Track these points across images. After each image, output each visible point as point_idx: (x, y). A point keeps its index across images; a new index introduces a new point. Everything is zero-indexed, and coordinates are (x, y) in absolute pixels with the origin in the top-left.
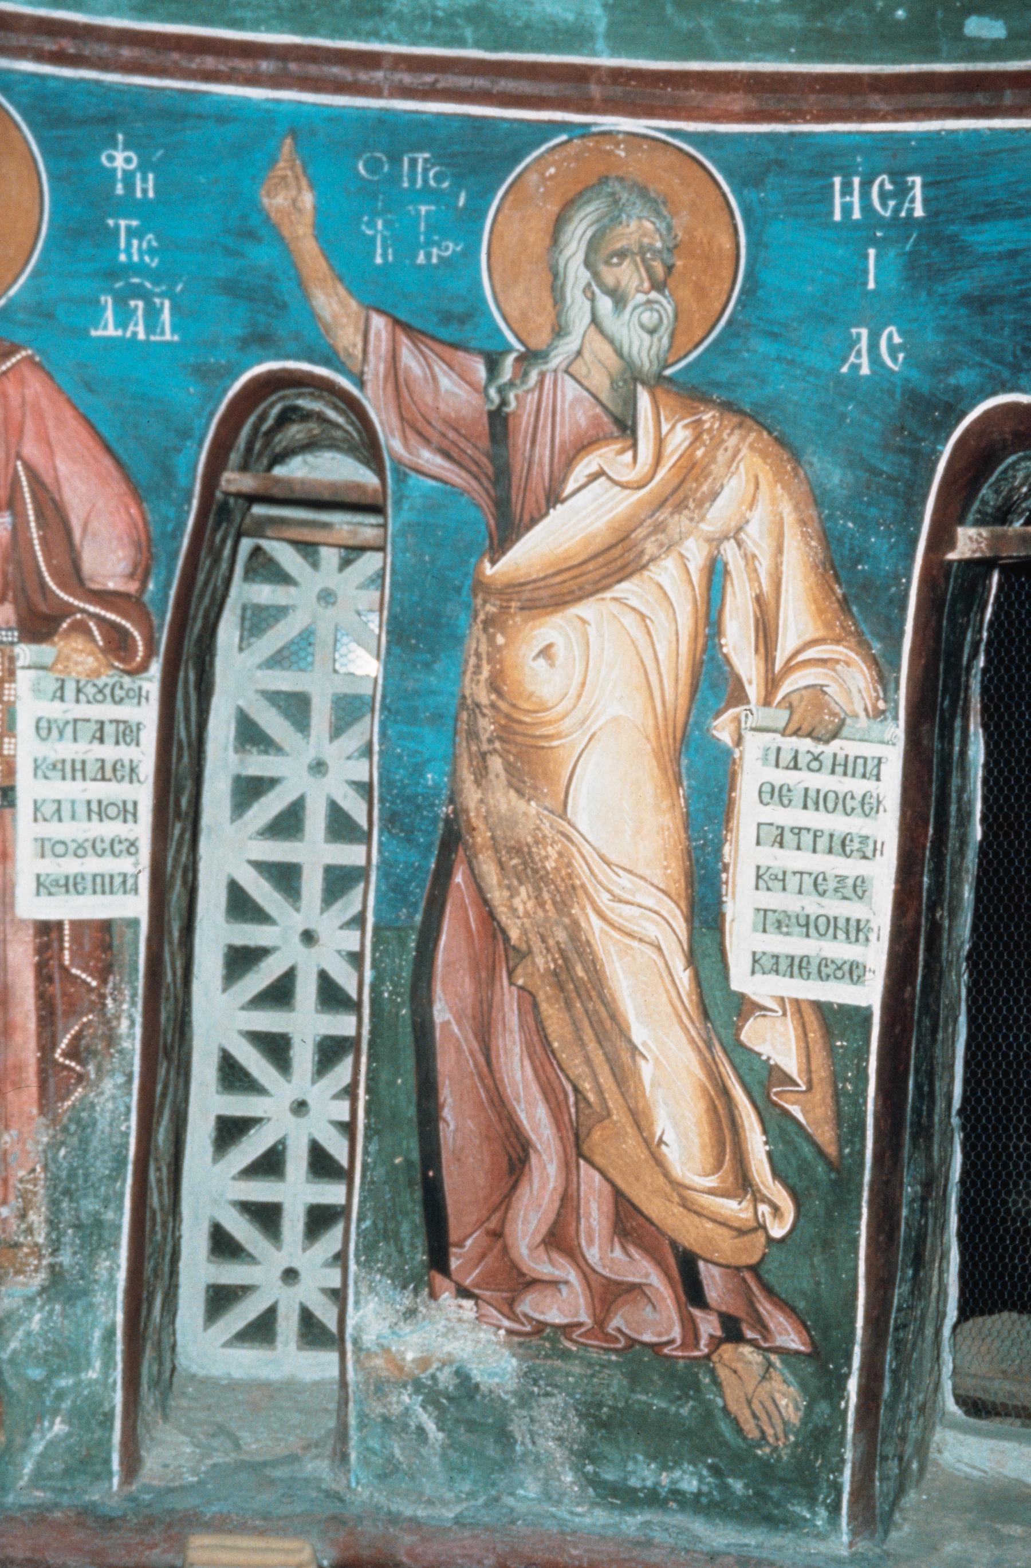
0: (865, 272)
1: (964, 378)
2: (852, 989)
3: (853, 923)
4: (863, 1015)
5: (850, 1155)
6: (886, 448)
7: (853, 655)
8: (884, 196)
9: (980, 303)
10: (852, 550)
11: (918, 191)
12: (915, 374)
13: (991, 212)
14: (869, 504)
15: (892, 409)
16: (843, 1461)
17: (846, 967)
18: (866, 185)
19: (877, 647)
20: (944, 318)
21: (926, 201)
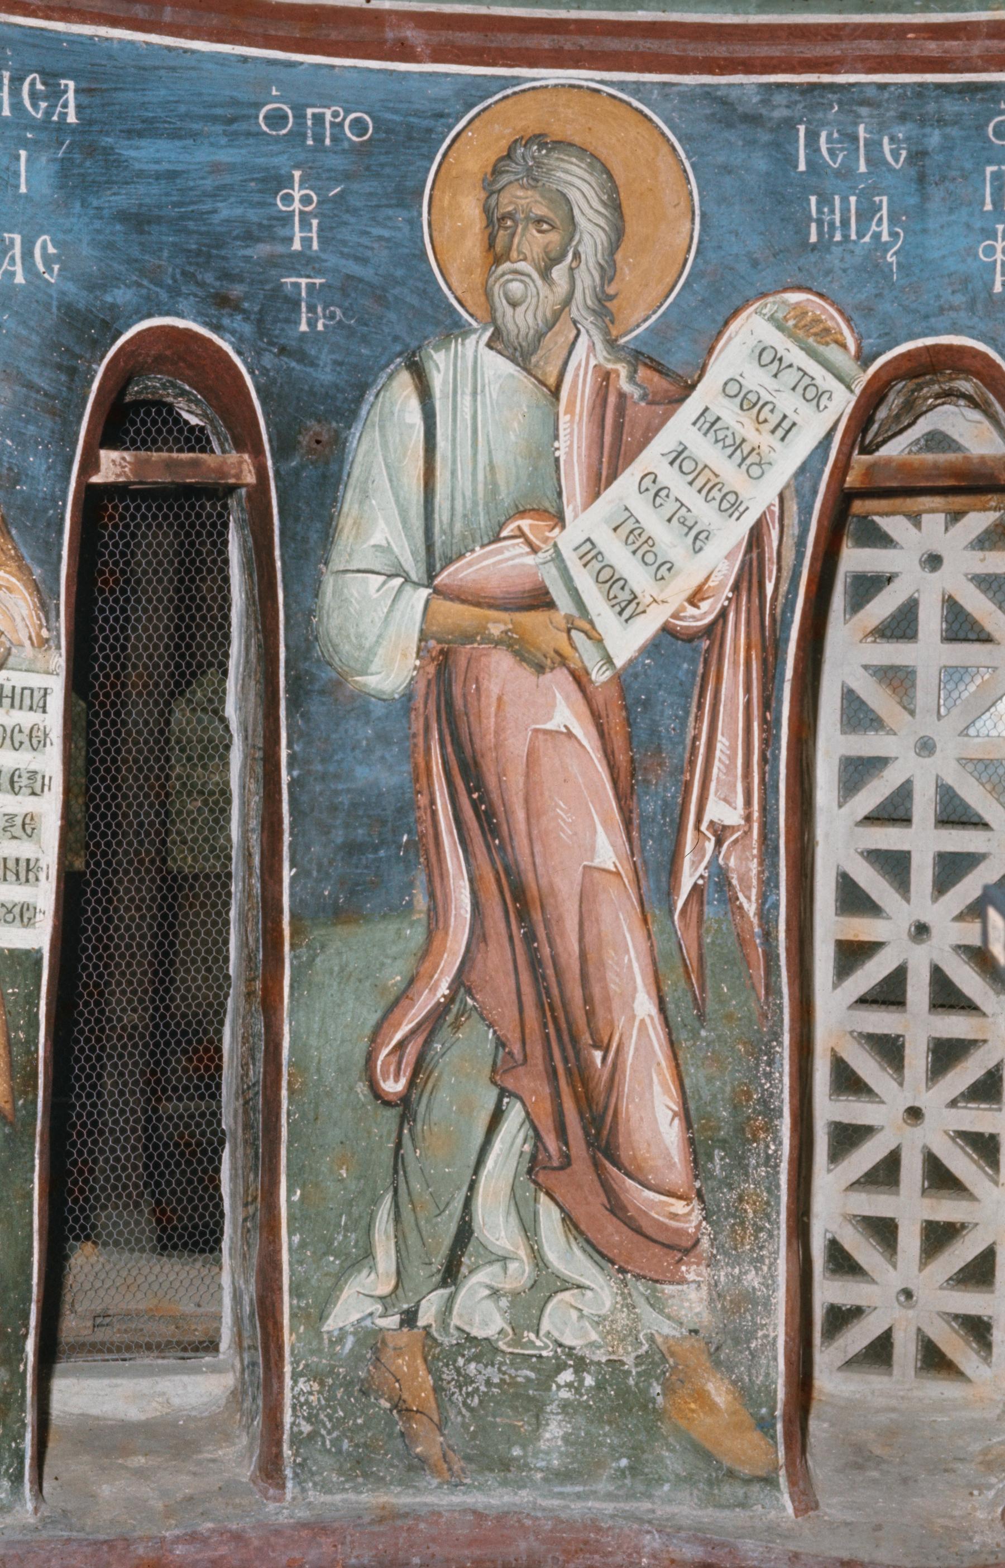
0: (17, 174)
1: (122, 296)
2: (23, 932)
3: (23, 864)
4: (33, 958)
5: (24, 1106)
6: (44, 363)
7: (14, 580)
8: (34, 95)
9: (137, 221)
10: (10, 469)
11: (71, 95)
12: (71, 287)
13: (147, 129)
14: (27, 421)
15: (48, 323)
16: (24, 1425)
17: (17, 910)
18: (17, 81)
19: (37, 572)
20: (98, 232)
21: (79, 108)
